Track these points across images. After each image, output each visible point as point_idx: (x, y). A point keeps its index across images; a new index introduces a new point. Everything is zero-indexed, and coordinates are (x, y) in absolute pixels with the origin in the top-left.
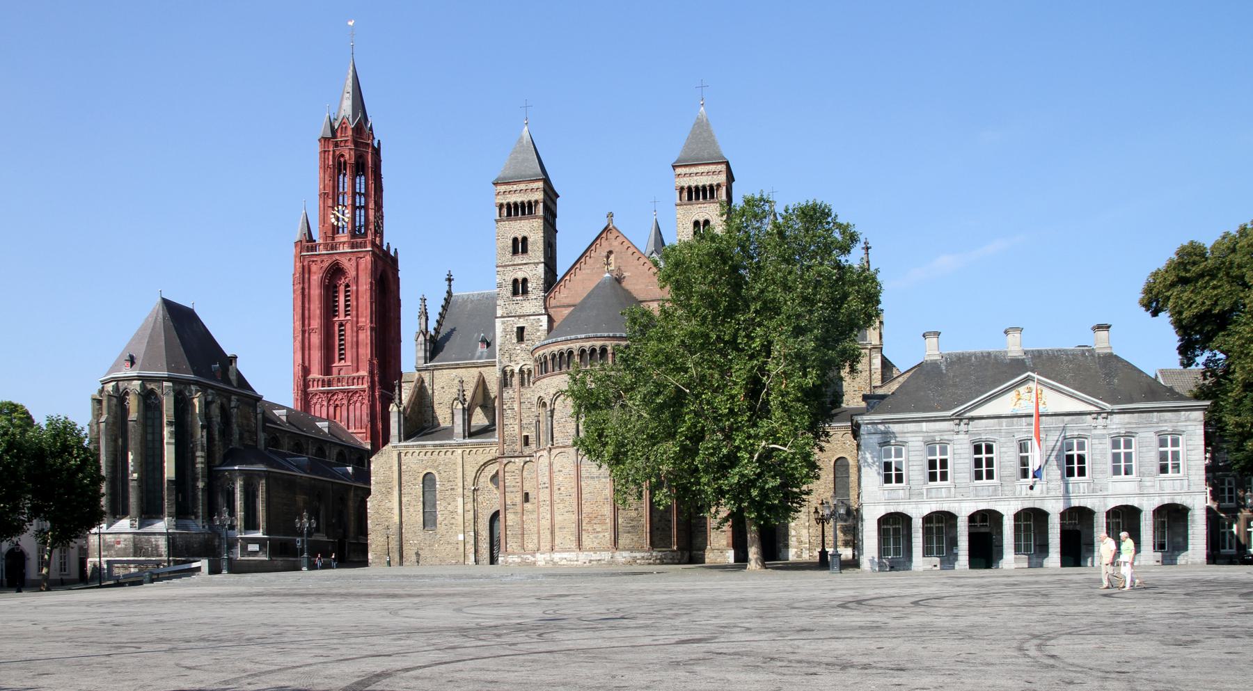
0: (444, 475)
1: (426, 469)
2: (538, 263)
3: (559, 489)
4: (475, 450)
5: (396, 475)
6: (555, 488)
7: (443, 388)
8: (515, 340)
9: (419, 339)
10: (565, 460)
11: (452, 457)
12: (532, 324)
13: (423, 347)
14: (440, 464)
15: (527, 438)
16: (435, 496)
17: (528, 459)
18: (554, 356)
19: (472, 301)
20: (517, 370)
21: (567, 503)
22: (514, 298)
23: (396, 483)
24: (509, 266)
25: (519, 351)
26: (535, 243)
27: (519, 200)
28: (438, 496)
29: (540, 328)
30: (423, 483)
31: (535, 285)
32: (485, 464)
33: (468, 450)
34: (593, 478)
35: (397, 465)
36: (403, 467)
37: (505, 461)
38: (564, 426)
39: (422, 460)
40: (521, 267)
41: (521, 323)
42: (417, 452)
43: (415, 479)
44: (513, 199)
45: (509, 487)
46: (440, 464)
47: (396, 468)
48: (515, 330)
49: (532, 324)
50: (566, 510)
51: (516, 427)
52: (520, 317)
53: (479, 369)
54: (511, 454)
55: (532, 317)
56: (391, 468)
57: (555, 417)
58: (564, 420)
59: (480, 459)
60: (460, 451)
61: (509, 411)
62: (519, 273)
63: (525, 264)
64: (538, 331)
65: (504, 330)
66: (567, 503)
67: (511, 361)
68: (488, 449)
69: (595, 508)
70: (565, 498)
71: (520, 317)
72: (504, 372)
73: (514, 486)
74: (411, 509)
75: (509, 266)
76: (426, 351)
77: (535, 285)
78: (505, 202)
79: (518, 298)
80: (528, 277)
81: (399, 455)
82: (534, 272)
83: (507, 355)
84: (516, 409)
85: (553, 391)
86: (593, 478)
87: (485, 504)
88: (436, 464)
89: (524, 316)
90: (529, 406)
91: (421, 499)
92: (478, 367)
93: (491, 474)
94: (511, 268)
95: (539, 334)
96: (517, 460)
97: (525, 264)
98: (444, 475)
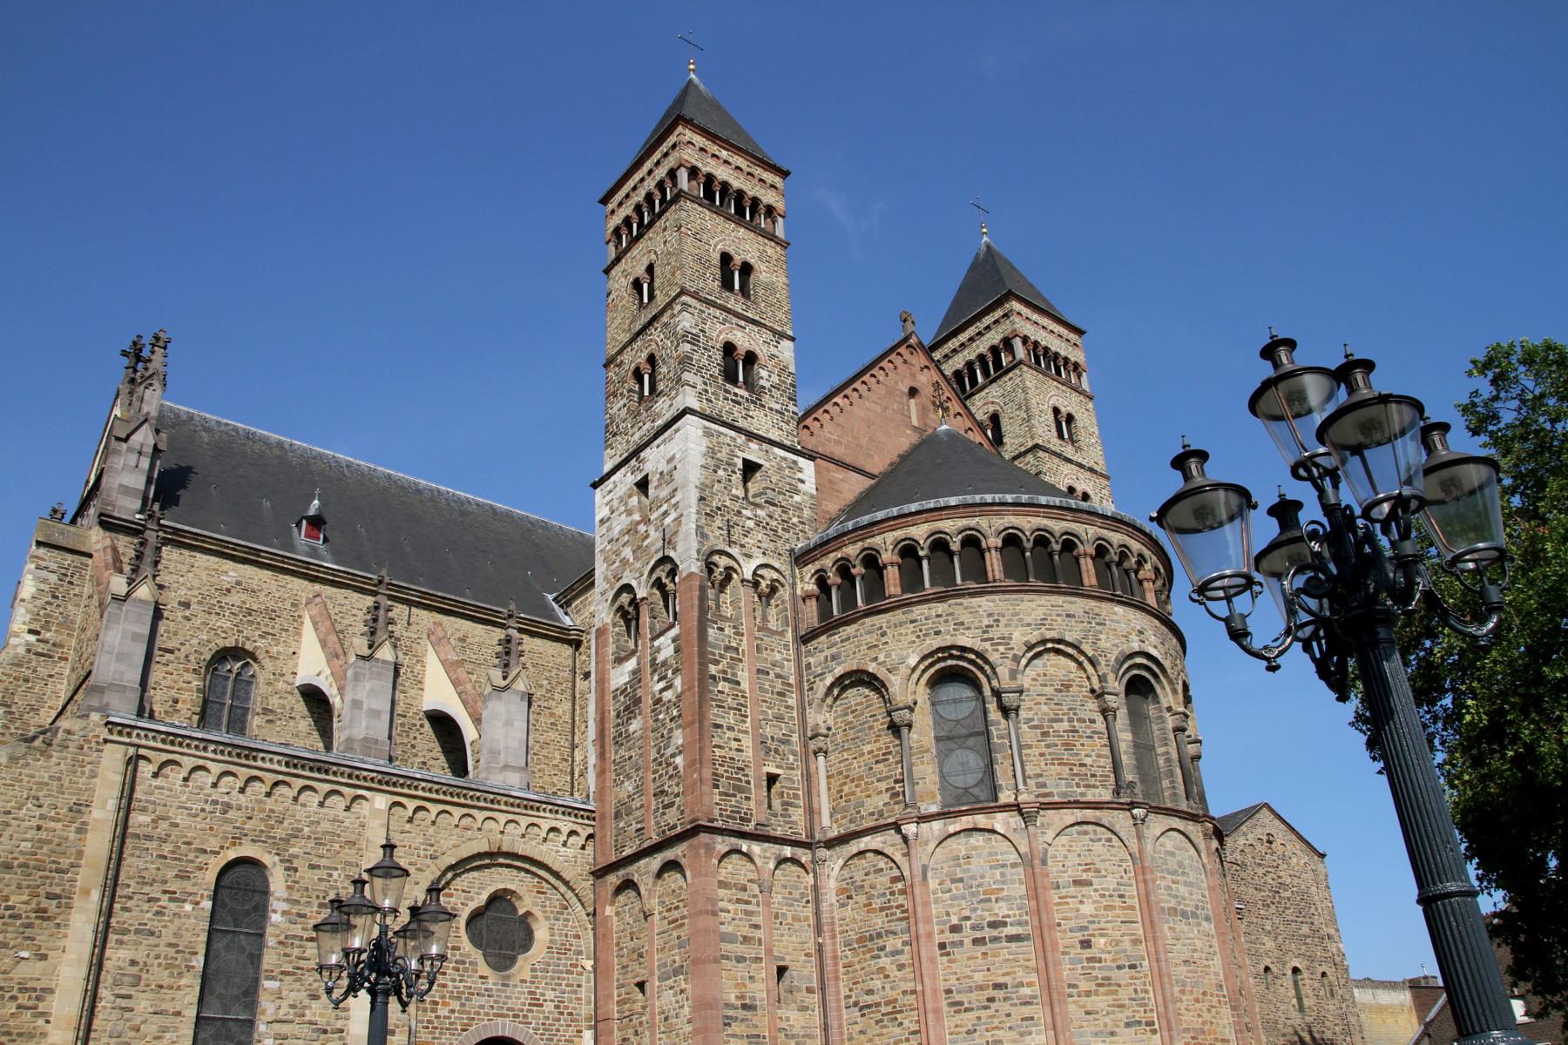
0: (306, 876)
1: (236, 841)
2: (782, 335)
3: (1086, 944)
4: (434, 809)
5: (98, 844)
6: (1067, 939)
7: (186, 605)
8: (740, 492)
9: (137, 438)
10: (1098, 848)
11: (349, 820)
12: (780, 468)
13: (145, 463)
14: (296, 834)
15: (772, 779)
16: (256, 959)
17: (787, 851)
18: (1011, 541)
19: (208, 430)
20: (748, 569)
21: (1124, 995)
22: (729, 386)
23: (90, 876)
24: (714, 305)
25: (750, 524)
26: (770, 288)
27: (736, 184)
28: (269, 959)
29: (800, 486)
30: (215, 898)
31: (775, 379)
32: (460, 867)
33: (411, 805)
34: (1184, 914)
35: (112, 804)
36: (138, 819)
37: (722, 844)
38: (1068, 746)
39: (227, 807)
40: (743, 323)
41: (754, 452)
42: (216, 769)
43: (183, 876)
44: (722, 173)
45: (727, 938)
46: (296, 834)
47: (103, 813)
48: (740, 464)
49: (780, 468)
50: (1123, 1016)
51: (747, 742)
52: (751, 436)
53: (317, 587)
54: (733, 825)
55: (776, 450)
56: (78, 808)
57: (1023, 714)
58: (1065, 725)
59: (446, 845)
60: (381, 801)
61: (722, 685)
62: (739, 334)
63: (754, 322)
64: (797, 492)
65: (711, 452)
66: (1124, 995)
67: (731, 543)
68: (480, 815)
69: (1207, 1016)
70: (1115, 974)
71: (751, 436)
72: (710, 567)
73: (746, 940)
74: (143, 1003)
75: (714, 305)
76: (149, 481)
77: (775, 379)
78: (705, 169)
79: (737, 390)
80: (758, 352)
81: (133, 762)
82: (773, 351)
83: (718, 522)
84: (745, 685)
85: (1019, 637)
86: (1184, 914)
87: (443, 1012)
88: (279, 832)
89: (761, 439)
90: (779, 687)
91: (198, 962)
92: (314, 579)
93: (473, 905)
94: (718, 313)
95: (797, 498)
96: (756, 848)
97: (754, 322)
98: (304, 874)
